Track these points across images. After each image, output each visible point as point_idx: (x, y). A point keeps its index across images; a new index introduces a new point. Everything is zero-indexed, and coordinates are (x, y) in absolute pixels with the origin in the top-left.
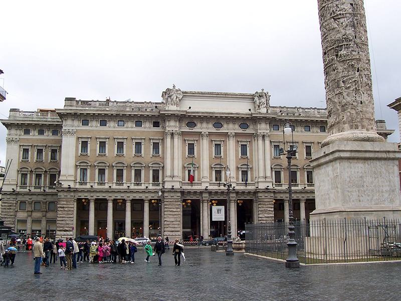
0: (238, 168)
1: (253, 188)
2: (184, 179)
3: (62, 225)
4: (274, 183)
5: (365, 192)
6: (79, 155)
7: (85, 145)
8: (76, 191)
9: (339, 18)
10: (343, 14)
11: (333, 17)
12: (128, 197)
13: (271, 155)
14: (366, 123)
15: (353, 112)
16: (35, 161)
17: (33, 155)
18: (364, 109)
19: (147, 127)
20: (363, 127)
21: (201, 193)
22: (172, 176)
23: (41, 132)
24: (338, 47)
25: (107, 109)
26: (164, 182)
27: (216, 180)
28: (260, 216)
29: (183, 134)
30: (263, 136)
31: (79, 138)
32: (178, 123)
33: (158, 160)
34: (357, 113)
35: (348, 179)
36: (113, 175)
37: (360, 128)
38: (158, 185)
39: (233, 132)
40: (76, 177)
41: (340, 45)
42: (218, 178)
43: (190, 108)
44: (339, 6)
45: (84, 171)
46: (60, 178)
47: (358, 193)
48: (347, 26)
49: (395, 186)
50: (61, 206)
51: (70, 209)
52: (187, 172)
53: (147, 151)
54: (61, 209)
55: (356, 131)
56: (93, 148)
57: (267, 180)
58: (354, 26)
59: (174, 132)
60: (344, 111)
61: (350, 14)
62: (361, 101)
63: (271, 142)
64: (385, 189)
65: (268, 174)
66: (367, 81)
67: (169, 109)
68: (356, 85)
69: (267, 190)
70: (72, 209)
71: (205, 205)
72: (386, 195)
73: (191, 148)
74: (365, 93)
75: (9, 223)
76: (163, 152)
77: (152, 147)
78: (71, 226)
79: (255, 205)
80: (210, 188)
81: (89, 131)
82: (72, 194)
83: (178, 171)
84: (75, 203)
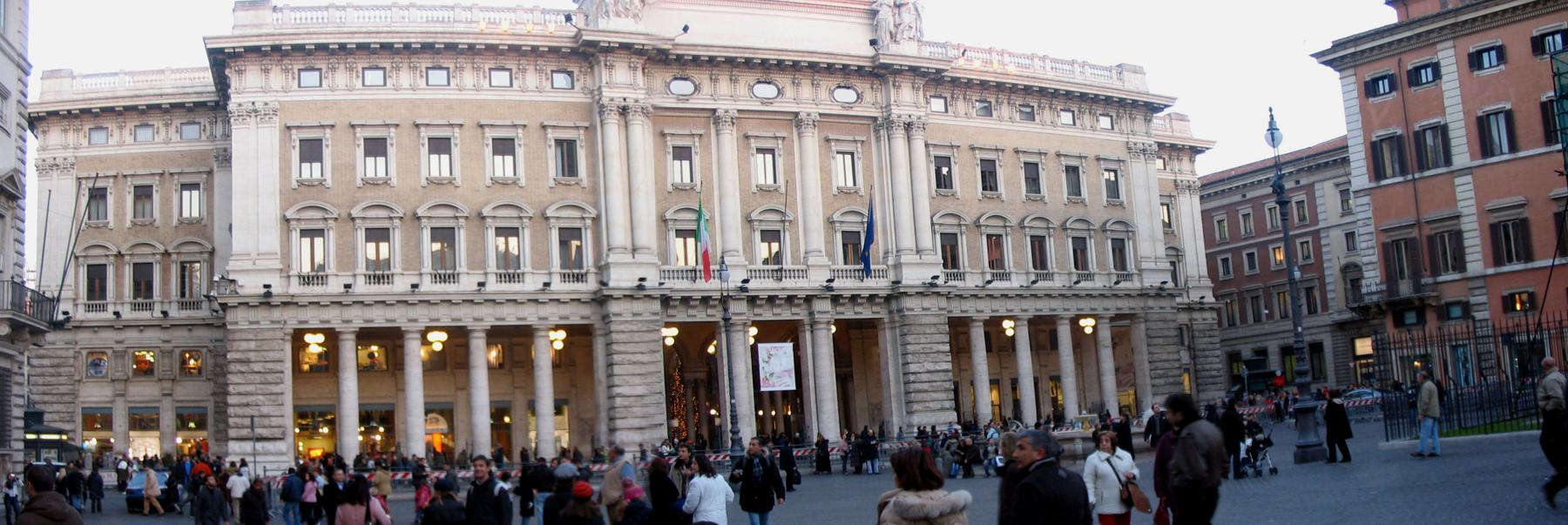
0: (830, 222)
12: (476, 320)
21: (724, 300)
22: (629, 246)
26: (602, 268)
28: (913, 368)
29: (658, 115)
30: (908, 127)
33: (574, 197)
38: (580, 278)
39: (815, 111)
50: (238, 356)
51: (270, 366)
54: (239, 367)
57: (926, 258)
59: (630, 103)
63: (927, 145)
65: (927, 240)
67: (611, 27)
69: (929, 289)
76: (593, 172)
79: (887, 338)
82: (277, 314)
83: (648, 234)
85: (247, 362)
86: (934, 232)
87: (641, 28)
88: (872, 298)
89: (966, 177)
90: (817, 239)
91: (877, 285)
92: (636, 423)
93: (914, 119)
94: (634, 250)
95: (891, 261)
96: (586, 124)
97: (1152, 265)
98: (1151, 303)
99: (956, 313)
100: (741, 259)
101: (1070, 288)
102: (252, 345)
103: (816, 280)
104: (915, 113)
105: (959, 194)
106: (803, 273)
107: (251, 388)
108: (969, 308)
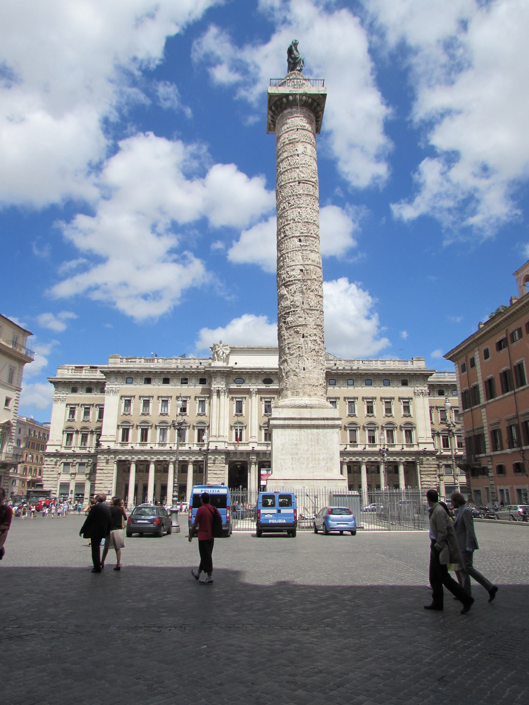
2: (230, 439)
3: (100, 489)
5: (299, 459)
7: (128, 403)
8: (116, 452)
9: (289, 285)
10: (292, 281)
11: (284, 284)
14: (308, 389)
15: (295, 378)
16: (81, 420)
17: (80, 413)
18: (307, 375)
20: (304, 393)
22: (217, 435)
24: (286, 314)
25: (152, 366)
27: (266, 440)
32: (224, 380)
33: (203, 418)
34: (298, 379)
35: (281, 447)
36: (156, 434)
37: (301, 394)
41: (288, 311)
43: (236, 363)
44: (289, 273)
45: (126, 432)
47: (291, 460)
48: (295, 292)
49: (334, 454)
52: (234, 431)
53: (193, 408)
55: (296, 398)
56: (137, 406)
58: (302, 292)
59: (220, 389)
60: (287, 377)
61: (299, 280)
62: (304, 368)
64: (321, 457)
66: (313, 346)
68: (299, 351)
70: (111, 471)
71: (253, 467)
72: (323, 463)
73: (239, 405)
74: (309, 359)
75: (51, 486)
78: (109, 489)
80: (258, 448)
84: (115, 466)
85: (103, 470)
87: (225, 365)
96: (208, 395)
97: (424, 441)
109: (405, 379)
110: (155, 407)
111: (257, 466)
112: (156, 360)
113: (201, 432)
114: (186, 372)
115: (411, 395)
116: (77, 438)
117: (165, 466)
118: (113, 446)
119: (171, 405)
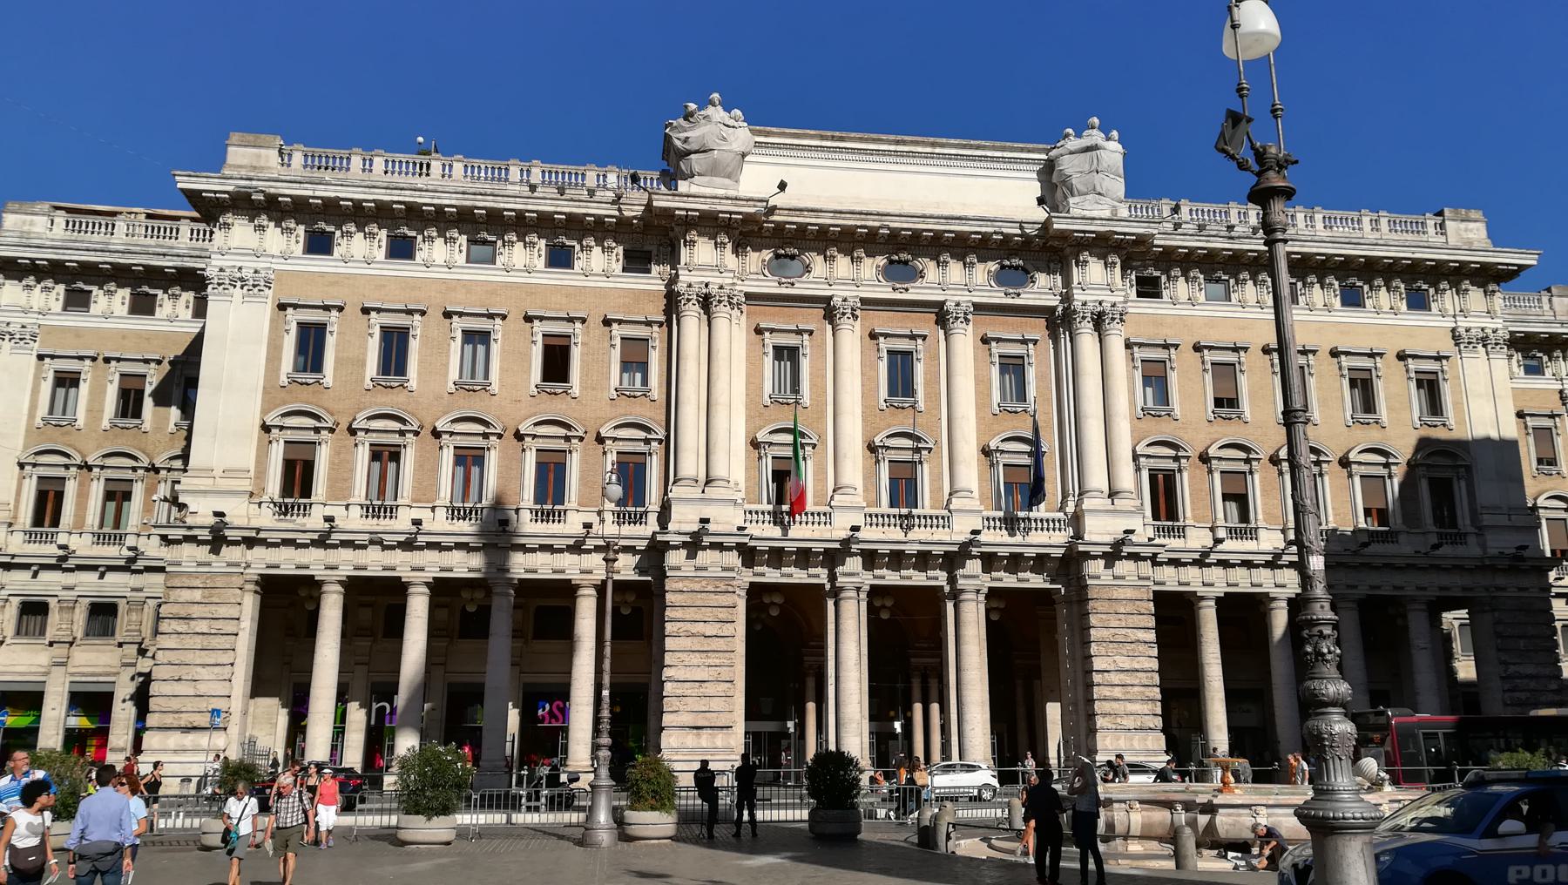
1: (1061, 537)
3: (175, 704)
4: (1149, 520)
6: (284, 380)
13: (1132, 402)
19: (599, 264)
22: (702, 477)
23: (142, 306)
30: (1099, 321)
31: (282, 307)
36: (436, 469)
38: (639, 519)
40: (261, 472)
42: (904, 489)
43: (782, 186)
46: (187, 482)
59: (713, 289)
65: (1126, 477)
67: (694, 190)
70: (230, 627)
77: (616, 355)
81: (337, 280)
83: (734, 463)
86: (1138, 469)
88: (1041, 563)
89: (1191, 390)
90: (970, 473)
91: (1054, 540)
92: (687, 719)
93: (1107, 306)
94: (708, 482)
95: (1070, 508)
97: (1503, 520)
98: (1501, 580)
99: (1172, 586)
100: (859, 500)
101: (1355, 553)
102: (197, 595)
103: (959, 531)
104: (1109, 299)
105: (1177, 412)
106: (946, 521)
107: (189, 657)
108: (1192, 579)
109: (1421, 280)
110: (436, 362)
111: (864, 605)
112: (436, 166)
113: (631, 473)
114: (569, 215)
115: (1447, 347)
116: (83, 496)
117: (471, 608)
118: (241, 514)
119: (503, 350)
